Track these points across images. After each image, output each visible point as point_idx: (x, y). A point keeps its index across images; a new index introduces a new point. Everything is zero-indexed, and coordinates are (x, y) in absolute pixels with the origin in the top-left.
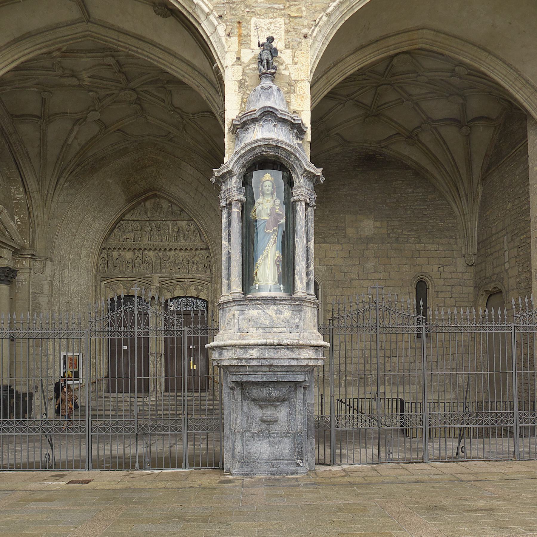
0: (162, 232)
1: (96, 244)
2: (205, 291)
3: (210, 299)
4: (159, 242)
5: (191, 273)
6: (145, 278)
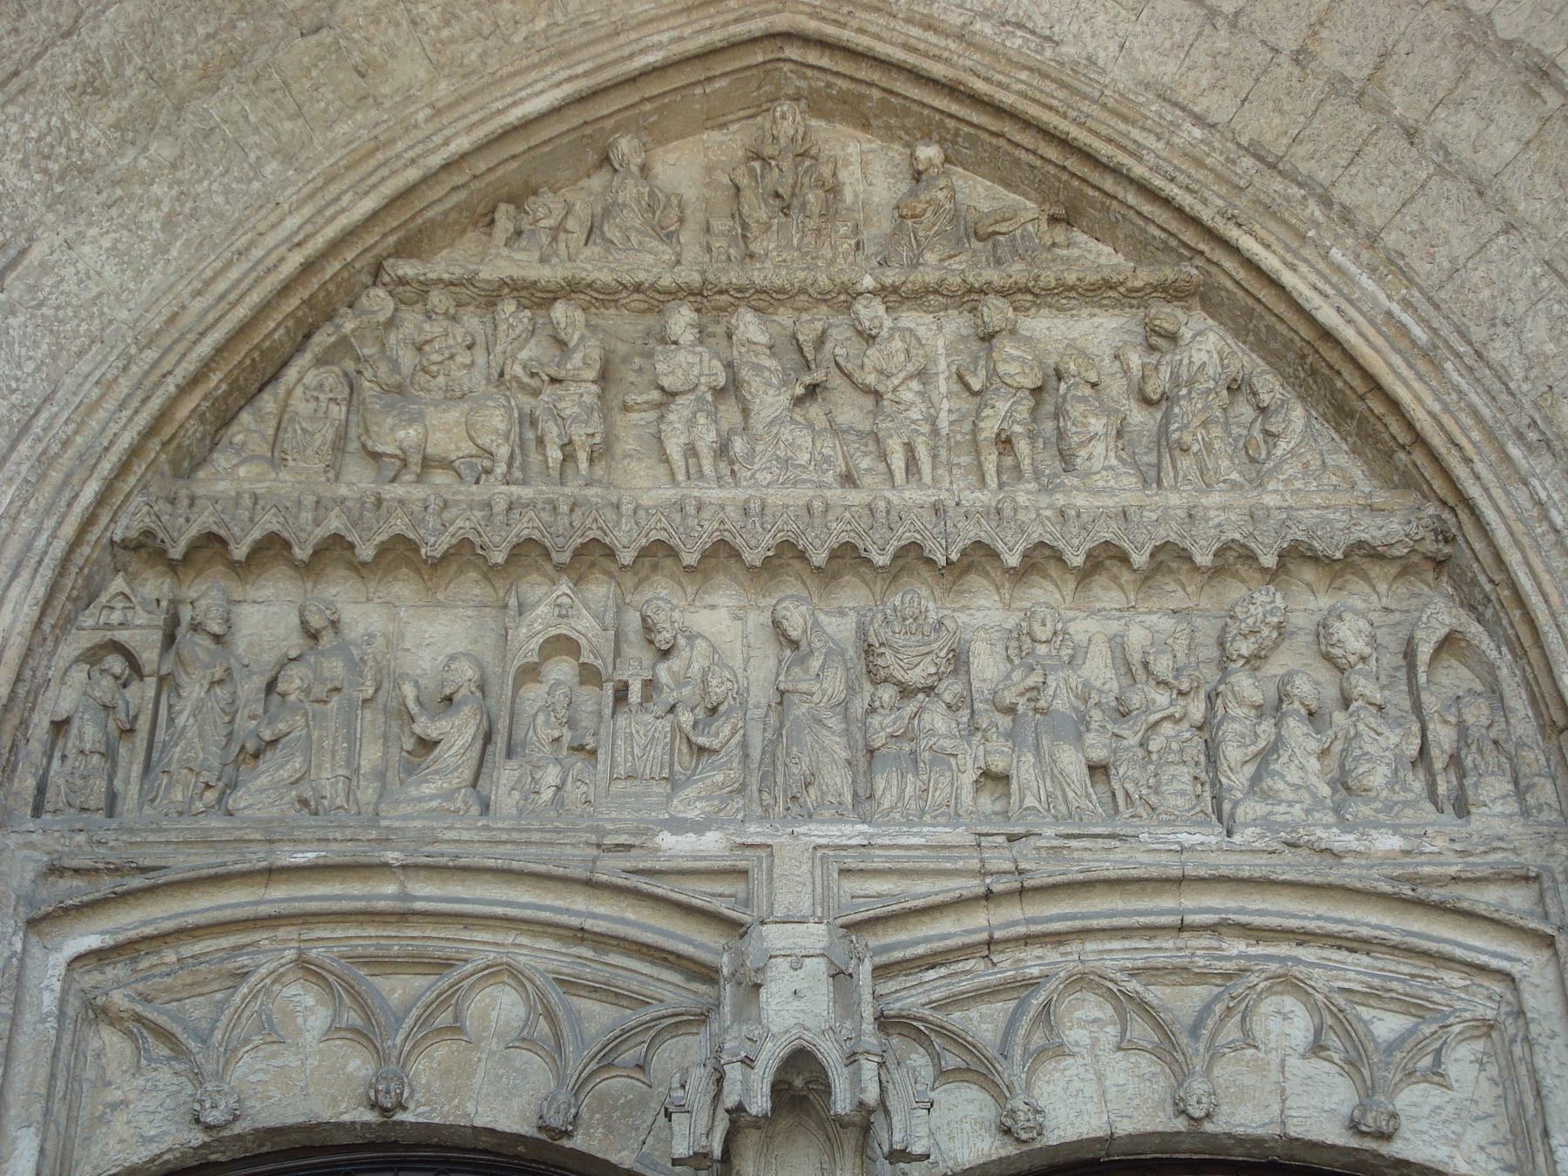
1: (44, 462)
2: (1462, 1060)
5: (1267, 823)
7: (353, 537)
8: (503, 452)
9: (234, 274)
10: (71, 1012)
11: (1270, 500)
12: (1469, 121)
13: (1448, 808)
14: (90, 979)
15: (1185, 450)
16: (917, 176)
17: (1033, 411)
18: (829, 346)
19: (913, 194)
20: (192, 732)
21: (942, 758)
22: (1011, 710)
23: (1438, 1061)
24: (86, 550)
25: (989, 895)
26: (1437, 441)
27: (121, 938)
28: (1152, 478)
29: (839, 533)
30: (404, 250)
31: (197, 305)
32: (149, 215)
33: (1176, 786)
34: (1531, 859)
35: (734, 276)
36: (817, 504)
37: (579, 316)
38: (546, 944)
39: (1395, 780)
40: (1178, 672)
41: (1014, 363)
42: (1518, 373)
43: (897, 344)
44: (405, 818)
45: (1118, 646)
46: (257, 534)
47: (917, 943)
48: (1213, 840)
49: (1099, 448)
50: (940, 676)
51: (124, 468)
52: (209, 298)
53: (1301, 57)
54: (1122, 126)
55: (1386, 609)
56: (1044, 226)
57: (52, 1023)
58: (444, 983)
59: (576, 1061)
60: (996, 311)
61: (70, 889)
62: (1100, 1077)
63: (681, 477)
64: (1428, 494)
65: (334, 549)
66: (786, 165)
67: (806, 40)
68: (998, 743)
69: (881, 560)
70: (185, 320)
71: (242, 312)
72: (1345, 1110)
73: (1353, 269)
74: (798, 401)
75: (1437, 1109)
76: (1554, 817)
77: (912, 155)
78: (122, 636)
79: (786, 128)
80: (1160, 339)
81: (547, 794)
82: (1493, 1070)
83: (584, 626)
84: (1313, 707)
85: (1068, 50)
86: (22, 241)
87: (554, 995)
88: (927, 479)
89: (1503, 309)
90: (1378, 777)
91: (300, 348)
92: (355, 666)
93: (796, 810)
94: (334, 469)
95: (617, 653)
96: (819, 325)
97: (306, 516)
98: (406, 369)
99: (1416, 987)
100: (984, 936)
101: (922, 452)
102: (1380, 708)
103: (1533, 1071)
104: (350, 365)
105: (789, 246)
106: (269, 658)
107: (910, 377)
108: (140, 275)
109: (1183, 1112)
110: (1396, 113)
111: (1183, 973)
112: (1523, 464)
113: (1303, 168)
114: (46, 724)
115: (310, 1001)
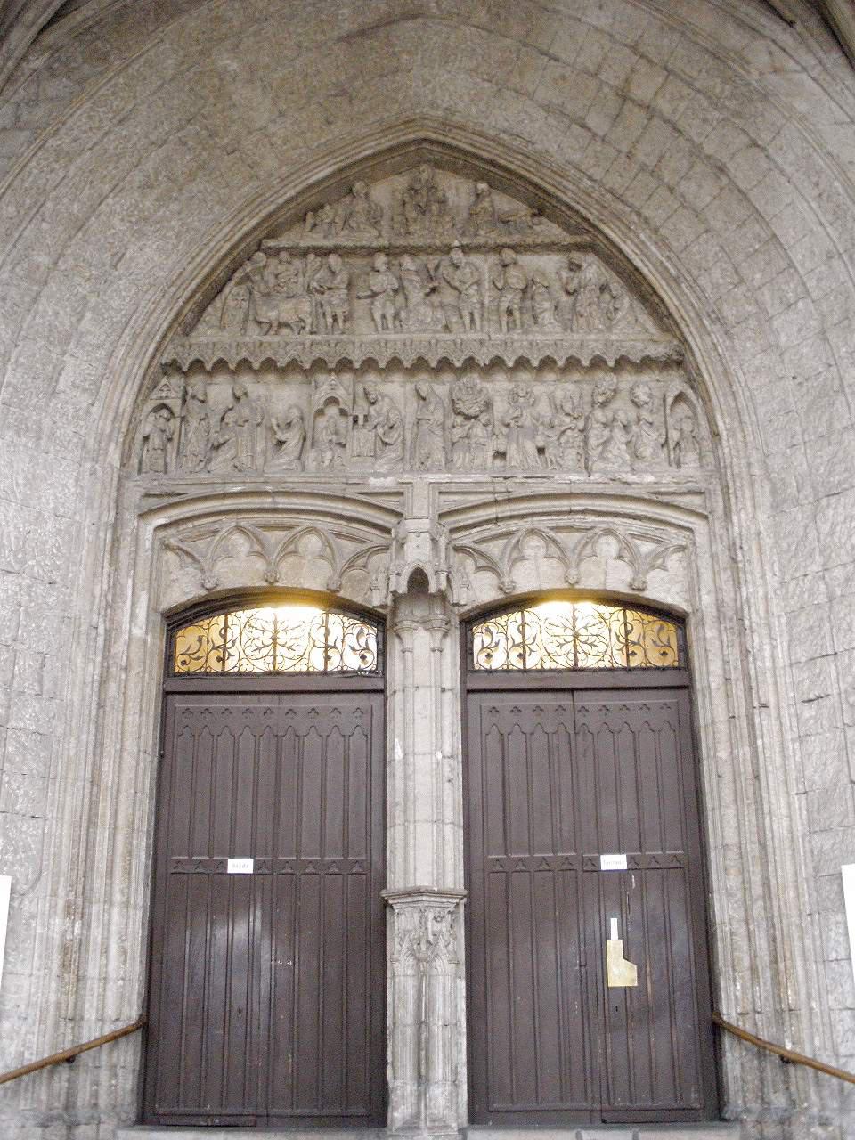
0: (448, 296)
1: (135, 336)
2: (674, 561)
3: (707, 600)
4: (436, 332)
5: (604, 472)
6: (366, 499)
7: (251, 359)
8: (309, 321)
9: (204, 253)
10: (156, 547)
11: (613, 337)
12: (694, 187)
13: (674, 465)
14: (162, 534)
15: (582, 316)
16: (478, 195)
17: (522, 299)
18: (441, 268)
19: (476, 204)
20: (193, 440)
21: (480, 446)
22: (508, 425)
23: (664, 561)
24: (152, 369)
25: (496, 502)
26: (677, 316)
27: (173, 519)
28: (567, 327)
29: (441, 353)
30: (270, 236)
31: (191, 267)
32: (170, 234)
33: (570, 457)
34: (702, 486)
35: (401, 242)
36: (433, 341)
37: (340, 260)
38: (328, 519)
39: (655, 453)
40: (574, 408)
41: (515, 278)
42: (709, 290)
43: (468, 270)
44: (274, 473)
45: (552, 399)
46: (215, 359)
47: (467, 519)
48: (582, 478)
49: (547, 315)
50: (482, 412)
51: (164, 337)
52: (195, 264)
53: (629, 156)
54: (558, 179)
55: (658, 381)
56: (529, 218)
57: (149, 552)
58: (290, 535)
59: (341, 563)
60: (508, 255)
61: (153, 503)
62: (538, 568)
63: (380, 329)
64: (675, 336)
65: (244, 365)
66: (424, 193)
67: (432, 142)
68: (502, 440)
69: (458, 365)
70: (186, 274)
71: (207, 269)
72: (629, 580)
73: (649, 244)
74: (427, 295)
75: (662, 579)
76: (713, 468)
77: (476, 187)
78: (167, 402)
79: (425, 176)
80: (575, 267)
81: (327, 463)
82: (685, 564)
83: (341, 393)
84: (626, 423)
85: (538, 147)
86: (123, 251)
87: (332, 538)
88: (478, 327)
89: (704, 263)
90: (647, 452)
91: (230, 279)
92: (253, 410)
93: (423, 467)
94: (244, 329)
95: (354, 402)
96: (436, 262)
97: (233, 351)
98: (271, 285)
99: (658, 533)
100: (494, 516)
101: (477, 316)
102: (651, 424)
103: (697, 566)
104: (250, 284)
105: (424, 228)
106: (222, 408)
107: (472, 284)
108: (168, 257)
109: (567, 581)
110: (666, 180)
111: (570, 529)
112: (709, 328)
113: (630, 200)
114: (141, 438)
115: (242, 541)
